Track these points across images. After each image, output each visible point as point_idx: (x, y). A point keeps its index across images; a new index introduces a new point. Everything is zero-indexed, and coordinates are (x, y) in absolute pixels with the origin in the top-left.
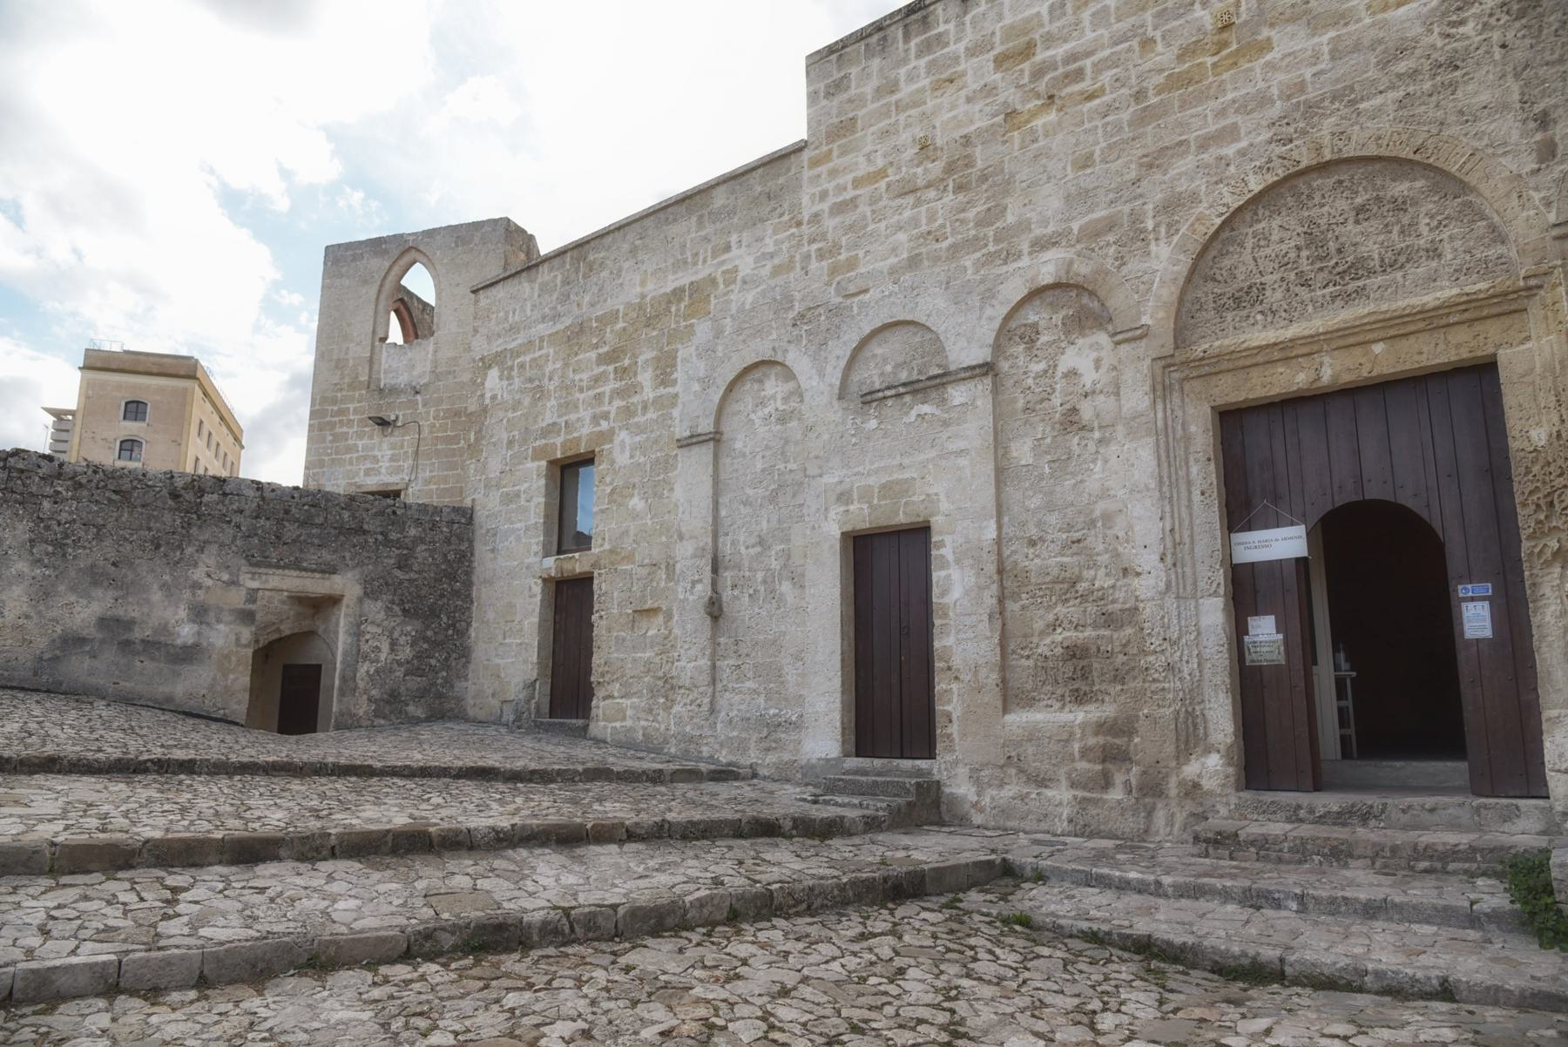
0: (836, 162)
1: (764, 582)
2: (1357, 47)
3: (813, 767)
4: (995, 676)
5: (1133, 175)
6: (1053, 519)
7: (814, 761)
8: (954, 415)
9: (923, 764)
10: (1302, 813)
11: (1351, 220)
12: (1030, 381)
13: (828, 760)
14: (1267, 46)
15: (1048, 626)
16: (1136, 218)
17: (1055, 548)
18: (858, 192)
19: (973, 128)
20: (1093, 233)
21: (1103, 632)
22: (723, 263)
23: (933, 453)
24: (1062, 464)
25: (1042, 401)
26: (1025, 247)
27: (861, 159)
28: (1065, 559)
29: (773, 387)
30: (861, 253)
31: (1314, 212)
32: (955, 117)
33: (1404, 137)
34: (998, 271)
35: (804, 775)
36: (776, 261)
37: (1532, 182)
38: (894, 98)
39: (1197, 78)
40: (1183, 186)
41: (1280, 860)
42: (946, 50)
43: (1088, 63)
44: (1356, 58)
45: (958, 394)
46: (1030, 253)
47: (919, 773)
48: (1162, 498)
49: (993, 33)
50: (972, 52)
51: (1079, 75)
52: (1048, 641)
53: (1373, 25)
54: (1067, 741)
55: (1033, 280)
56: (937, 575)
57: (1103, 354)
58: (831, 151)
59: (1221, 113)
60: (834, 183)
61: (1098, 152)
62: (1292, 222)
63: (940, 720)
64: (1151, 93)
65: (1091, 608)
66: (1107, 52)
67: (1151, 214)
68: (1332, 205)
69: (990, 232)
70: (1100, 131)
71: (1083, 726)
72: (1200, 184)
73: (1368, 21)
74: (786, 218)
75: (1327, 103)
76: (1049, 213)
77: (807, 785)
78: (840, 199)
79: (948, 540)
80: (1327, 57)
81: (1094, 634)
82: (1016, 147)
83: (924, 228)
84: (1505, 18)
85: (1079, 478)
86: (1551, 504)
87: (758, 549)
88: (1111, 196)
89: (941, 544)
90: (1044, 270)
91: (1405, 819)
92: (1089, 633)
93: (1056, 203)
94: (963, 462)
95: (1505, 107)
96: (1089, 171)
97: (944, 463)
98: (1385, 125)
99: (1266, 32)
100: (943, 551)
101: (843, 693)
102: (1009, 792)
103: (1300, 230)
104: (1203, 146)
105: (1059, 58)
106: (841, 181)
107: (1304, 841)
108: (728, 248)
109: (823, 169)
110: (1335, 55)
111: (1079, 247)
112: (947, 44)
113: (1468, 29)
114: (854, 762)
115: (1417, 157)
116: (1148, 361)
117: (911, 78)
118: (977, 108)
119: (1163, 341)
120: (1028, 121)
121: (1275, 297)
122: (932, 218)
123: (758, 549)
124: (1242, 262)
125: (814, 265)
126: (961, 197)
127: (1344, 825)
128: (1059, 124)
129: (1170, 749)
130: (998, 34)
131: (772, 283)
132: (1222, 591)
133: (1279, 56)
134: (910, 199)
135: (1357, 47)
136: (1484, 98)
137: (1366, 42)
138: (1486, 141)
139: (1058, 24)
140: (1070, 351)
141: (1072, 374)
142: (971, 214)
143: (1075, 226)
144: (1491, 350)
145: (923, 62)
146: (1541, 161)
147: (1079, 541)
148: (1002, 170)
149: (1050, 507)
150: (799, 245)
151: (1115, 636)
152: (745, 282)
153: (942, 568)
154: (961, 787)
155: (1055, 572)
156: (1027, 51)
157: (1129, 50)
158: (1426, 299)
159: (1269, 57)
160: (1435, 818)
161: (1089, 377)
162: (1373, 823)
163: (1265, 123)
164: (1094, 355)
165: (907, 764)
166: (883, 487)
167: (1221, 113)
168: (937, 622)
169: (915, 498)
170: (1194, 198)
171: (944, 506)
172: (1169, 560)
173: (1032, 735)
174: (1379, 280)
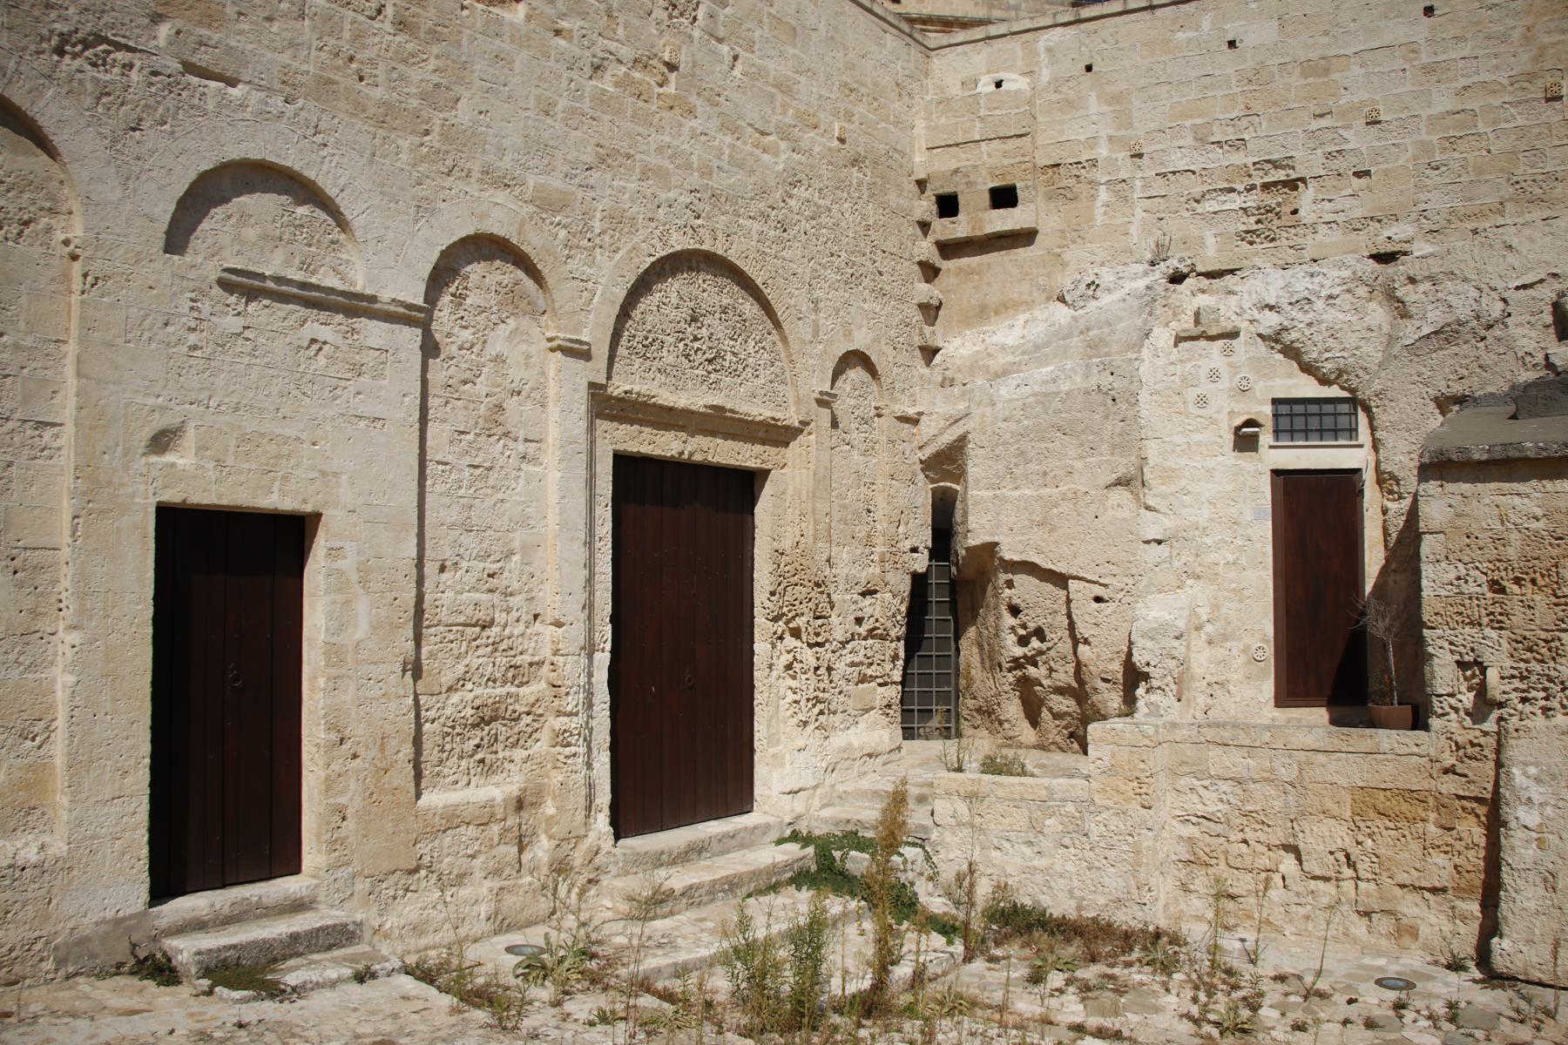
3: (84, 941)
5: (589, 158)
6: (469, 540)
12: (454, 348)
13: (117, 922)
14: (691, 112)
17: (470, 579)
20: (548, 204)
25: (465, 383)
26: (477, 169)
35: (60, 962)
45: (374, 332)
52: (455, 698)
65: (502, 660)
67: (599, 215)
76: (506, 142)
85: (500, 496)
88: (566, 168)
90: (496, 213)
92: (501, 691)
122: (358, 36)
141: (498, 359)
142: (415, 74)
155: (469, 612)
161: (516, 373)
162: (704, 855)
163: (688, 187)
173: (452, 820)
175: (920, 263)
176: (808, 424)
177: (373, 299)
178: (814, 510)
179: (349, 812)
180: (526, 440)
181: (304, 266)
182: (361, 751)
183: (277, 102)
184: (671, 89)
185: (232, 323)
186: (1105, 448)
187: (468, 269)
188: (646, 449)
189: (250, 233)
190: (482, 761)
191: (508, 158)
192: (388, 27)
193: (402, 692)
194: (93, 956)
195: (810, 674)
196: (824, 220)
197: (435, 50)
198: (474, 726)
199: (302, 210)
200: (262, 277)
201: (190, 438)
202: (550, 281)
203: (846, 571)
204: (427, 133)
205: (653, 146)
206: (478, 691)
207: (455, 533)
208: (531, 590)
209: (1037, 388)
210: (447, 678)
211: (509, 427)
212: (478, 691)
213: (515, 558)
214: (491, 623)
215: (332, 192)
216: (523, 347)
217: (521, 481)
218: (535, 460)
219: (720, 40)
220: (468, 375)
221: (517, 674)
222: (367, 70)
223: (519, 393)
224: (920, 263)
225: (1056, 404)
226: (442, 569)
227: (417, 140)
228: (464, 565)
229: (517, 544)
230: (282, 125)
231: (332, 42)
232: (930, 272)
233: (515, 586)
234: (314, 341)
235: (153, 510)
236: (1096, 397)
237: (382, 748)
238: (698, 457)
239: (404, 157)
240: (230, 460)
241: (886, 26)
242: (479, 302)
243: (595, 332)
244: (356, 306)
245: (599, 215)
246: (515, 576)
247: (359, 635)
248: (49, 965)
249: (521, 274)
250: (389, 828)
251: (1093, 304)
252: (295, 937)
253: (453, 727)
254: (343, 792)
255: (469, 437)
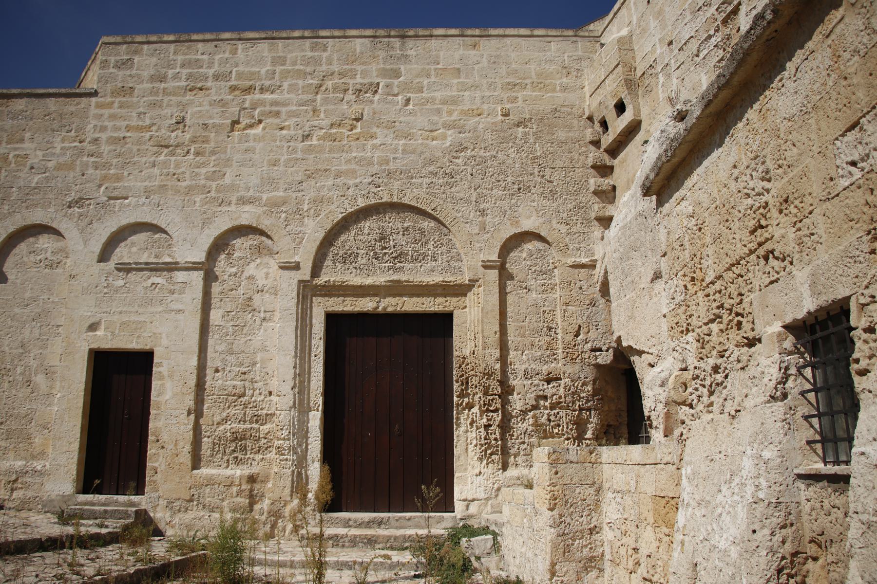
0: (115, 110)
1: (23, 374)
2: (413, 152)
4: (188, 447)
5: (299, 178)
6: (231, 359)
7: (53, 497)
8: (177, 287)
9: (135, 498)
10: (351, 523)
11: (401, 233)
12: (226, 277)
13: (63, 496)
15: (223, 420)
16: (299, 203)
17: (232, 375)
18: (128, 134)
19: (211, 121)
20: (274, 205)
21: (254, 426)
22: (16, 149)
23: (160, 309)
24: (239, 328)
25: (232, 290)
27: (134, 114)
28: (235, 382)
29: (45, 242)
30: (126, 174)
31: (386, 225)
32: (200, 112)
33: (429, 201)
34: (215, 209)
35: (44, 506)
36: (62, 160)
37: (476, 238)
38: (162, 86)
39: (339, 139)
40: (325, 192)
41: (343, 546)
42: (201, 70)
43: (284, 110)
44: (412, 157)
45: (180, 276)
46: (237, 204)
47: (132, 504)
48: (296, 356)
49: (231, 72)
50: (216, 77)
51: (277, 114)
52: (222, 428)
53: (422, 144)
54: (230, 486)
55: (236, 219)
56: (155, 384)
57: (271, 271)
58: (113, 103)
59: (348, 161)
60: (112, 124)
61: (282, 160)
62: (374, 225)
63: (149, 473)
64: (314, 138)
66: (294, 108)
67: (307, 202)
68: (393, 222)
69: (214, 185)
70: (285, 149)
71: (241, 477)
72: (334, 194)
73: (420, 141)
74: (73, 133)
75: (398, 173)
76: (251, 184)
77: (45, 512)
78: (116, 135)
79: (165, 363)
80: (400, 151)
81: (249, 426)
82: (236, 141)
83: (172, 170)
84: (473, 162)
85: (249, 338)
86: (467, 383)
87: (21, 351)
88: (286, 186)
89: (160, 364)
90: (244, 216)
91: (397, 524)
92: (248, 426)
93: (255, 180)
94: (180, 317)
95: (470, 202)
96: (276, 168)
97: (167, 316)
98: (422, 193)
99: (375, 129)
100: (161, 369)
101: (80, 452)
102: (190, 515)
103: (377, 231)
104: (338, 175)
105: (267, 101)
106: (118, 124)
107: (355, 536)
108: (22, 140)
109: (106, 112)
110: (404, 151)
111: (265, 208)
112: (202, 67)
113: (459, 161)
114: (82, 498)
115: (433, 213)
116: (296, 281)
117: (176, 77)
118: (215, 111)
119: (305, 273)
120: (244, 129)
121: (362, 261)
122: (177, 166)
123: (21, 351)
124: (347, 239)
125: (91, 171)
126: (198, 159)
127: (370, 528)
128: (263, 137)
129: (287, 491)
130: (234, 73)
131: (55, 173)
132: (320, 408)
133: (379, 143)
134: (166, 151)
135: (413, 152)
136: (461, 195)
137: (418, 151)
138: (460, 214)
139: (269, 82)
140: (253, 265)
141: (251, 278)
142: (203, 171)
143: (265, 197)
144: (452, 309)
145: (185, 71)
146: (480, 230)
147: (245, 373)
148: (226, 152)
149: (231, 352)
150: (80, 155)
151: (261, 428)
152: (32, 168)
153: (159, 379)
154: (160, 515)
155: (230, 389)
156: (249, 90)
157: (306, 111)
158: (429, 279)
159: (375, 141)
160: (409, 523)
161: (261, 282)
162: (383, 526)
164: (265, 270)
165: (122, 498)
166: (123, 323)
167: (348, 161)
168: (152, 412)
169: (145, 334)
170: (330, 201)
171: (165, 342)
172: (296, 390)
173: (210, 482)
174: (408, 266)
175: (592, 167)
176: (477, 281)
177: (177, 263)
178: (483, 331)
179: (159, 470)
180: (265, 312)
181: (156, 257)
182: (166, 446)
183: (143, 199)
184: (358, 130)
185: (121, 283)
186: (649, 253)
187: (234, 242)
188: (348, 309)
189: (134, 249)
190: (236, 457)
191: (251, 191)
192: (191, 157)
193: (186, 422)
194: (55, 507)
195: (482, 430)
196: (489, 163)
197: (213, 158)
198: (232, 441)
199: (157, 236)
200: (129, 264)
201: (103, 327)
202: (275, 238)
203: (524, 367)
204: (209, 192)
205: (343, 161)
206: (233, 425)
207: (223, 356)
208: (266, 380)
209: (621, 225)
210: (217, 418)
211: (255, 307)
212: (233, 425)
213: (258, 365)
214: (244, 395)
215: (163, 227)
216: (265, 270)
217: (262, 331)
218: (271, 320)
219: (396, 95)
220: (233, 287)
221: (258, 419)
222: (181, 176)
223: (262, 291)
224: (592, 167)
225: (628, 233)
226: (217, 371)
227: (204, 196)
228: (228, 369)
229: (258, 359)
230: (144, 208)
231: (165, 171)
232: (605, 170)
233: (258, 378)
234: (153, 284)
235: (87, 351)
236: (640, 219)
237: (176, 445)
238: (390, 309)
239: (197, 204)
240: (117, 332)
241: (549, 39)
242: (239, 255)
243: (305, 257)
244: (172, 267)
245: (307, 202)
246: (258, 374)
247: (167, 397)
248: (40, 506)
249: (264, 238)
250: (177, 480)
251: (646, 155)
252: (106, 511)
253: (220, 441)
254: (156, 461)
255: (233, 313)
